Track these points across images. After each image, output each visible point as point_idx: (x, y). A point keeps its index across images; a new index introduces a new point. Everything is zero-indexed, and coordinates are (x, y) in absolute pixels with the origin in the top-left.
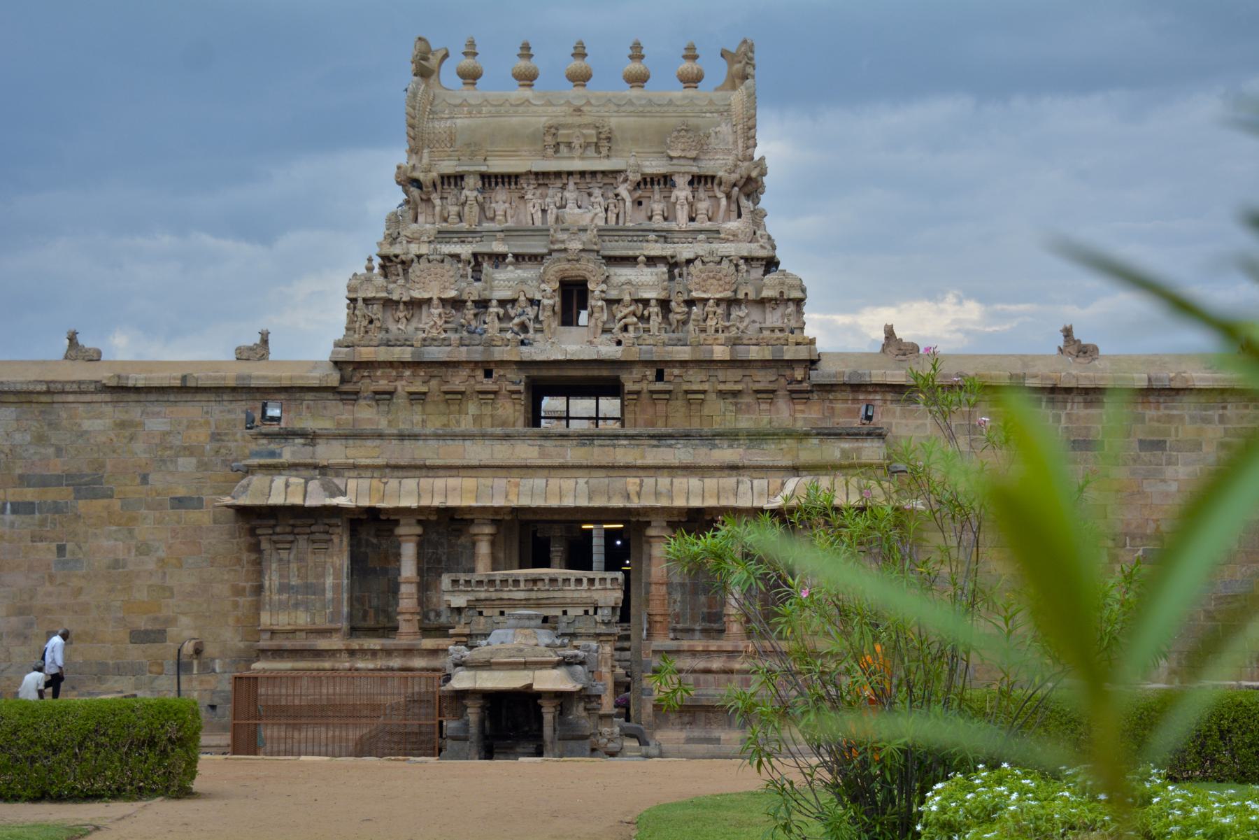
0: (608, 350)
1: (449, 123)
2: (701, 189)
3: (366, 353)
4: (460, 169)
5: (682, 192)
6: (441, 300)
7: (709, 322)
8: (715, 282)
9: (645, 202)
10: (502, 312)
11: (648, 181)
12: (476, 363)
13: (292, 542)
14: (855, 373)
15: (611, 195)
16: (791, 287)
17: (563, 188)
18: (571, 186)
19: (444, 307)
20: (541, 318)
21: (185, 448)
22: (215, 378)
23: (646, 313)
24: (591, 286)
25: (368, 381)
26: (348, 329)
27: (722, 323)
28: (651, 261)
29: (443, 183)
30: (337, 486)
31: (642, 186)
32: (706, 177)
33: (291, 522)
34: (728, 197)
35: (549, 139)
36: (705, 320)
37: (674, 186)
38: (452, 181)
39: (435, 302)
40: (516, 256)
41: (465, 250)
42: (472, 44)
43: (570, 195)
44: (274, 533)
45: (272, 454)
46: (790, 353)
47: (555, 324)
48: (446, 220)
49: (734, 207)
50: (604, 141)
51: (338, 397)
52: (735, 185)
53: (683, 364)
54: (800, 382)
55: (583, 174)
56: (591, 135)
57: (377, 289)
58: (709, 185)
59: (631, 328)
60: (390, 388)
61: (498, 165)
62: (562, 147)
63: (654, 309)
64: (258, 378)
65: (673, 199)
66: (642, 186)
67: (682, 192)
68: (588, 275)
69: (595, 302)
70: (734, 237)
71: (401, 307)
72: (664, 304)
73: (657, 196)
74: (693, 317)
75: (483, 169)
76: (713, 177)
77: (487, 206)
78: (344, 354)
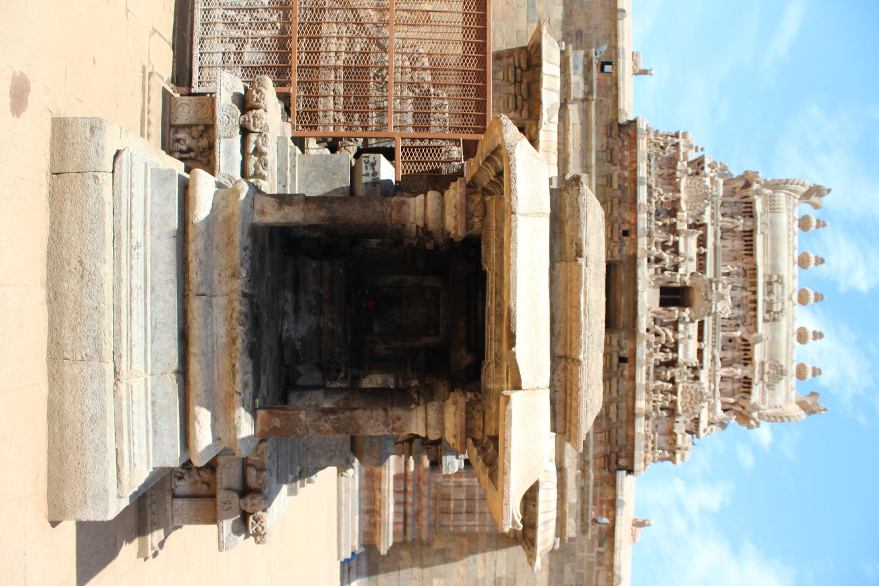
0: (644, 321)
1: (784, 207)
2: (742, 385)
3: (643, 145)
4: (759, 215)
5: (739, 372)
6: (679, 200)
7: (661, 396)
8: (688, 400)
9: (731, 344)
10: (670, 244)
11: (747, 346)
12: (636, 225)
13: (508, 80)
14: (623, 503)
15: (739, 322)
16: (683, 456)
17: (744, 288)
18: (745, 294)
19: (673, 201)
20: (666, 273)
21: (571, 11)
22: (623, 33)
23: (668, 350)
24: (687, 310)
25: (620, 144)
26: (657, 132)
27: (659, 404)
28: (700, 352)
29: (746, 203)
30: (553, 115)
31: (744, 343)
32: (750, 388)
33: (525, 81)
34: (733, 404)
35: (775, 278)
36: (661, 392)
37: (746, 364)
38: (748, 210)
39: (678, 195)
40: (705, 254)
41: (707, 219)
42: (824, 225)
43: (739, 294)
44: (516, 68)
45: (576, 68)
46: (639, 454)
47: (661, 283)
48: (722, 205)
49: (727, 407)
50: (773, 317)
51: (609, 122)
52: (743, 408)
53: (633, 378)
54: (617, 462)
55: (755, 301)
56: (777, 307)
57: (685, 154)
58: (743, 390)
59: (658, 338)
60: (616, 161)
61: (759, 240)
62: (770, 287)
63: (670, 356)
64: (624, 64)
65: (735, 365)
66: (744, 343)
67: (739, 372)
68: (696, 307)
69: (676, 310)
70: (712, 409)
71: (671, 171)
72: (672, 363)
73: (737, 354)
74: (665, 384)
75: (759, 232)
76: (749, 393)
77: (730, 234)
78: (642, 125)
